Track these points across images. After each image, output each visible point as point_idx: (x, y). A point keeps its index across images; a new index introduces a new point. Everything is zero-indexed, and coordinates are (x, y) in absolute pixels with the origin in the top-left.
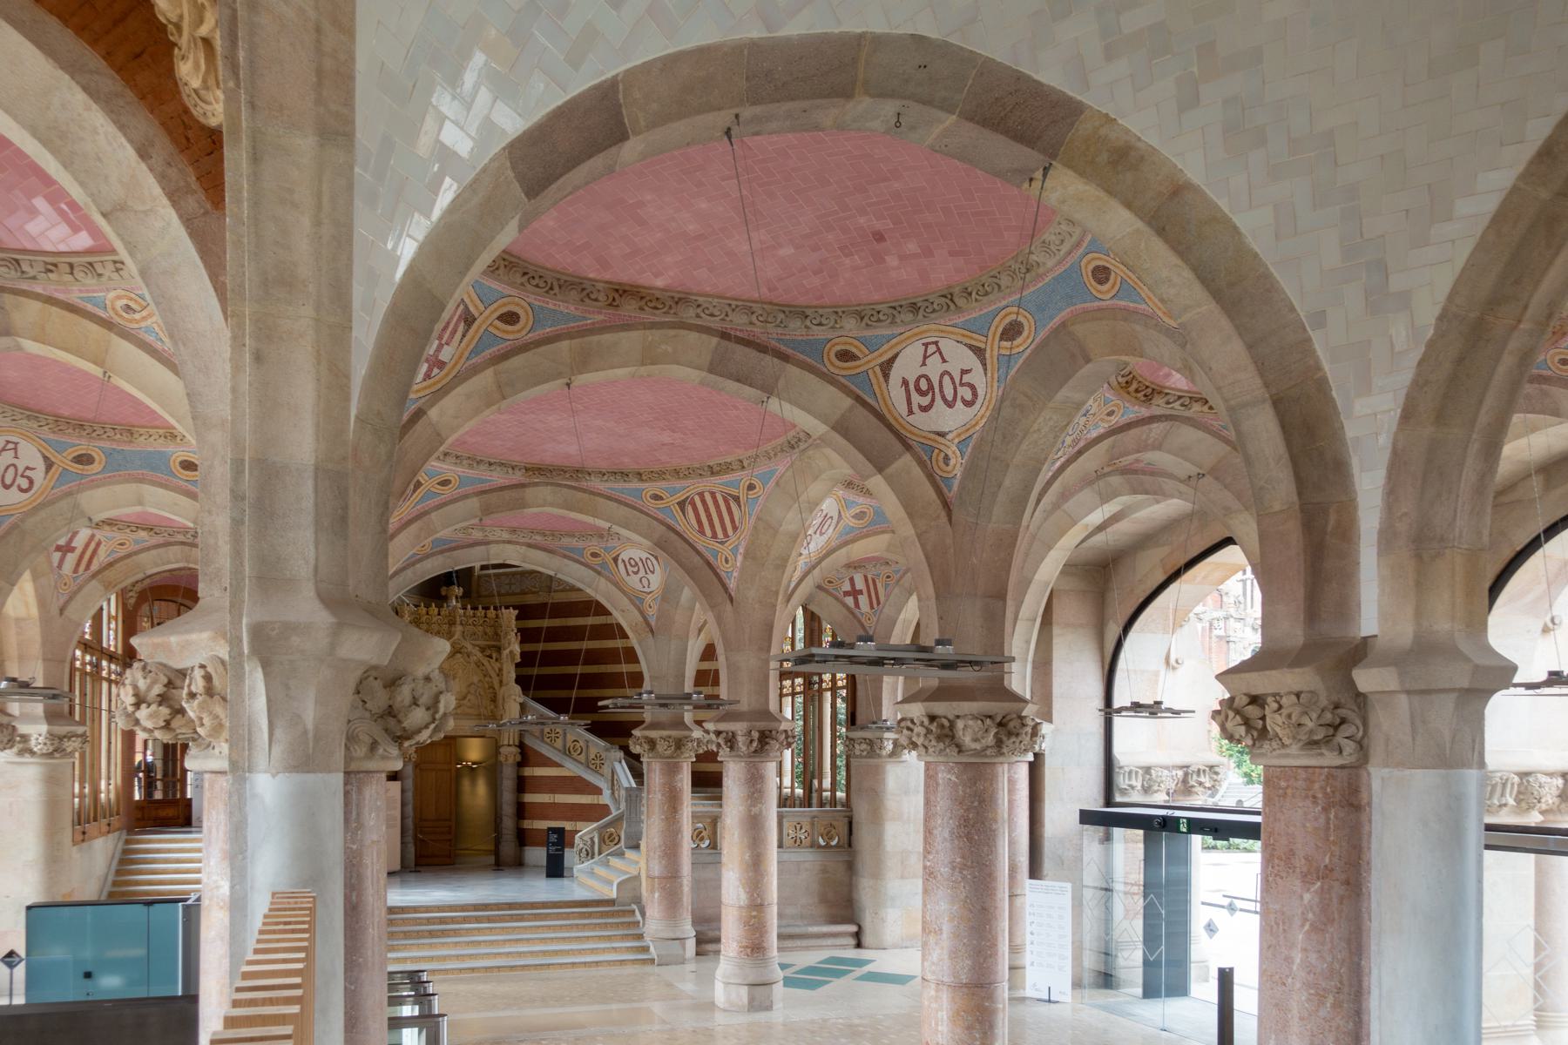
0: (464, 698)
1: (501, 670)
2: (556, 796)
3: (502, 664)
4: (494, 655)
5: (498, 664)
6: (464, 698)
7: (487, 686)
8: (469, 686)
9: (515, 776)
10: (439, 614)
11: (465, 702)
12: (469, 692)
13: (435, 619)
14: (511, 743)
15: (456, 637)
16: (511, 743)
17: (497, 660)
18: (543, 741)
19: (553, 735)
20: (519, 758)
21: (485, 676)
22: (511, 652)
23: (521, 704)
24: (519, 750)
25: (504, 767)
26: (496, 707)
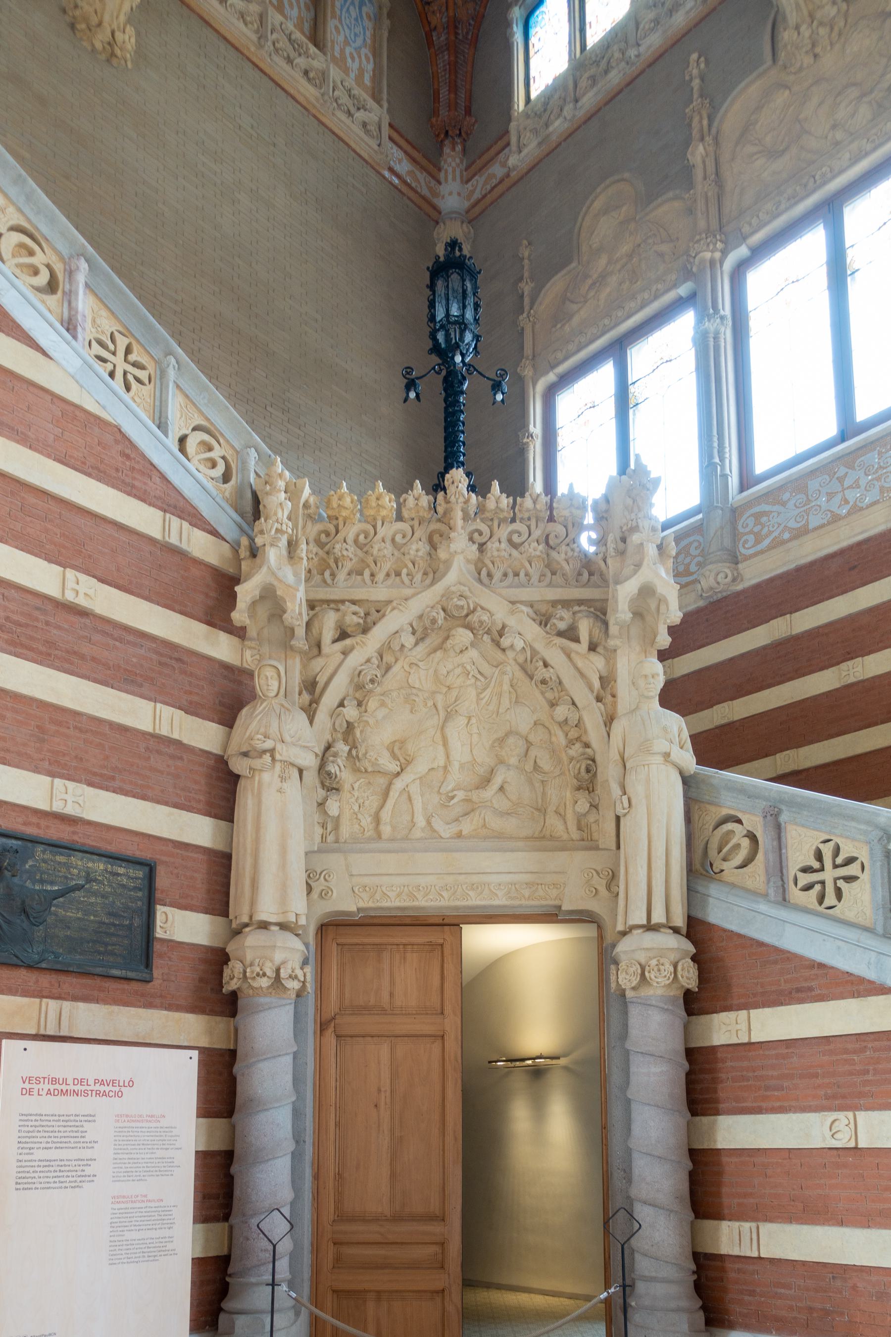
0: (485, 781)
1: (607, 681)
2: (863, 1117)
3: (611, 655)
4: (585, 627)
5: (596, 664)
6: (485, 781)
7: (560, 739)
8: (501, 741)
9: (681, 1049)
10: (400, 518)
11: (490, 792)
12: (501, 762)
13: (382, 532)
14: (658, 917)
15: (451, 577)
16: (658, 917)
17: (593, 648)
18: (784, 901)
19: (828, 875)
20: (689, 977)
21: (553, 705)
22: (647, 591)
23: (687, 781)
24: (692, 949)
25: (634, 1013)
26: (594, 806)
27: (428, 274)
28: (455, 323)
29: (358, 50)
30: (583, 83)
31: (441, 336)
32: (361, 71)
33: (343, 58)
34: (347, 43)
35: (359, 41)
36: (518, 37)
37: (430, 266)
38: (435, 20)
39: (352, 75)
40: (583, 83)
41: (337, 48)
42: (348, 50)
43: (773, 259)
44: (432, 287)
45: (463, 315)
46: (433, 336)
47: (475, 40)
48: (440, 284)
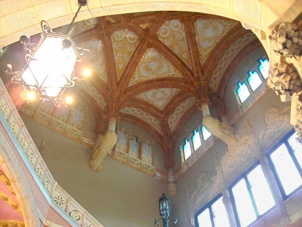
27: (159, 201)
28: (165, 209)
29: (149, 157)
30: (194, 157)
31: (162, 212)
32: (149, 161)
33: (145, 160)
34: (146, 157)
35: (149, 156)
36: (182, 149)
37: (159, 199)
38: (165, 149)
39: (147, 162)
40: (194, 157)
41: (144, 158)
42: (146, 158)
43: (235, 186)
44: (160, 203)
45: (166, 208)
46: (160, 213)
47: (173, 151)
48: (161, 202)
